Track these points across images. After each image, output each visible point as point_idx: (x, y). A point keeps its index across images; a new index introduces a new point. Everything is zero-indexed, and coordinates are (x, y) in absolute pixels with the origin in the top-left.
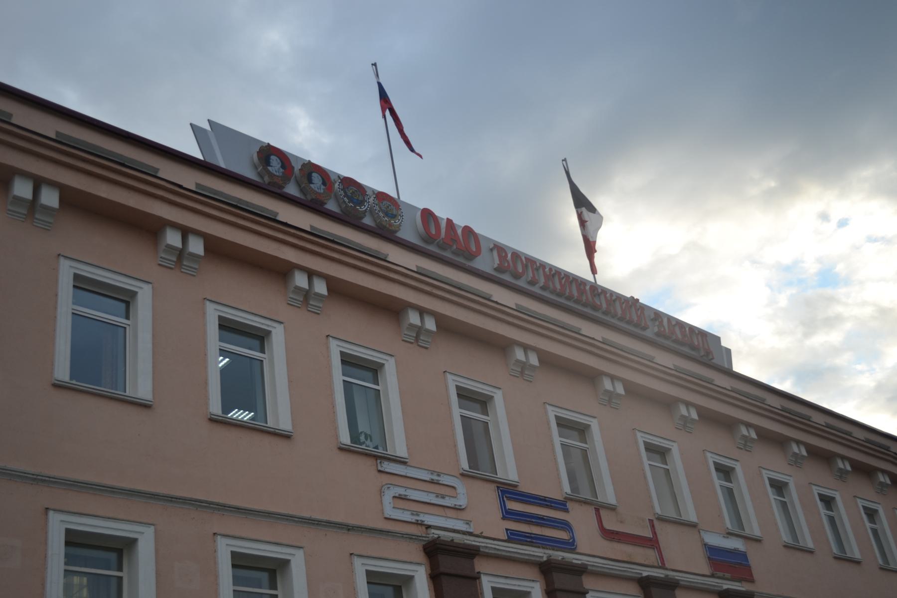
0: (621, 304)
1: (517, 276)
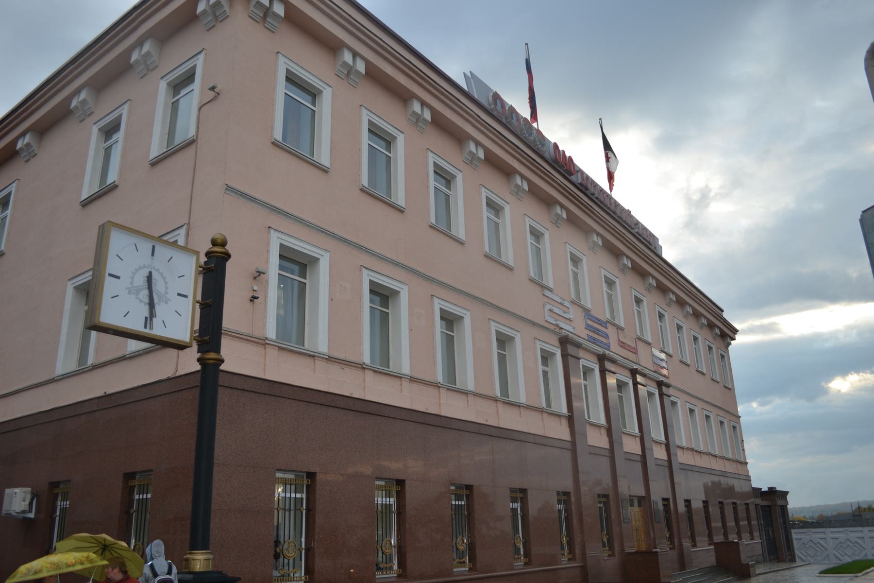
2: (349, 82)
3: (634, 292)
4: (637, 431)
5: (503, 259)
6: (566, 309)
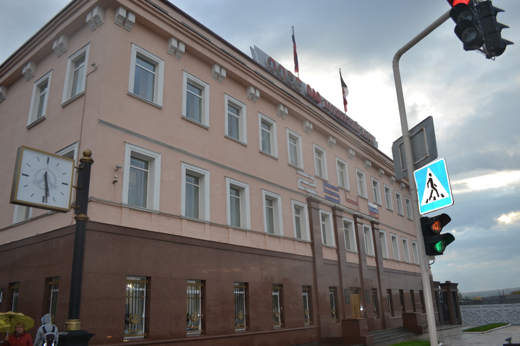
1: (328, 111)
2: (176, 57)
3: (357, 170)
4: (356, 250)
5: (272, 154)
6: (311, 181)
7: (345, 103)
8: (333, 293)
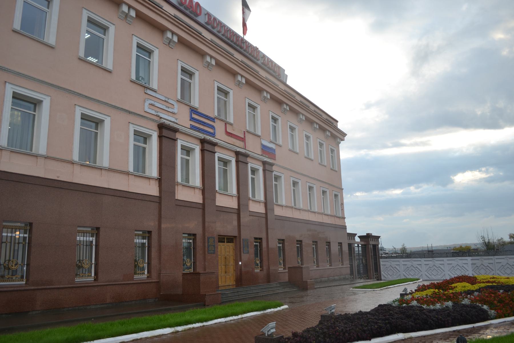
0: (251, 48)
1: (213, 28)
7: (244, 25)
8: (258, 244)
